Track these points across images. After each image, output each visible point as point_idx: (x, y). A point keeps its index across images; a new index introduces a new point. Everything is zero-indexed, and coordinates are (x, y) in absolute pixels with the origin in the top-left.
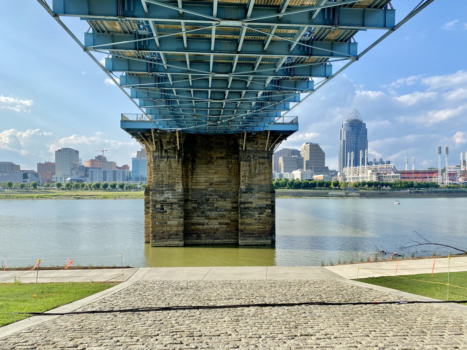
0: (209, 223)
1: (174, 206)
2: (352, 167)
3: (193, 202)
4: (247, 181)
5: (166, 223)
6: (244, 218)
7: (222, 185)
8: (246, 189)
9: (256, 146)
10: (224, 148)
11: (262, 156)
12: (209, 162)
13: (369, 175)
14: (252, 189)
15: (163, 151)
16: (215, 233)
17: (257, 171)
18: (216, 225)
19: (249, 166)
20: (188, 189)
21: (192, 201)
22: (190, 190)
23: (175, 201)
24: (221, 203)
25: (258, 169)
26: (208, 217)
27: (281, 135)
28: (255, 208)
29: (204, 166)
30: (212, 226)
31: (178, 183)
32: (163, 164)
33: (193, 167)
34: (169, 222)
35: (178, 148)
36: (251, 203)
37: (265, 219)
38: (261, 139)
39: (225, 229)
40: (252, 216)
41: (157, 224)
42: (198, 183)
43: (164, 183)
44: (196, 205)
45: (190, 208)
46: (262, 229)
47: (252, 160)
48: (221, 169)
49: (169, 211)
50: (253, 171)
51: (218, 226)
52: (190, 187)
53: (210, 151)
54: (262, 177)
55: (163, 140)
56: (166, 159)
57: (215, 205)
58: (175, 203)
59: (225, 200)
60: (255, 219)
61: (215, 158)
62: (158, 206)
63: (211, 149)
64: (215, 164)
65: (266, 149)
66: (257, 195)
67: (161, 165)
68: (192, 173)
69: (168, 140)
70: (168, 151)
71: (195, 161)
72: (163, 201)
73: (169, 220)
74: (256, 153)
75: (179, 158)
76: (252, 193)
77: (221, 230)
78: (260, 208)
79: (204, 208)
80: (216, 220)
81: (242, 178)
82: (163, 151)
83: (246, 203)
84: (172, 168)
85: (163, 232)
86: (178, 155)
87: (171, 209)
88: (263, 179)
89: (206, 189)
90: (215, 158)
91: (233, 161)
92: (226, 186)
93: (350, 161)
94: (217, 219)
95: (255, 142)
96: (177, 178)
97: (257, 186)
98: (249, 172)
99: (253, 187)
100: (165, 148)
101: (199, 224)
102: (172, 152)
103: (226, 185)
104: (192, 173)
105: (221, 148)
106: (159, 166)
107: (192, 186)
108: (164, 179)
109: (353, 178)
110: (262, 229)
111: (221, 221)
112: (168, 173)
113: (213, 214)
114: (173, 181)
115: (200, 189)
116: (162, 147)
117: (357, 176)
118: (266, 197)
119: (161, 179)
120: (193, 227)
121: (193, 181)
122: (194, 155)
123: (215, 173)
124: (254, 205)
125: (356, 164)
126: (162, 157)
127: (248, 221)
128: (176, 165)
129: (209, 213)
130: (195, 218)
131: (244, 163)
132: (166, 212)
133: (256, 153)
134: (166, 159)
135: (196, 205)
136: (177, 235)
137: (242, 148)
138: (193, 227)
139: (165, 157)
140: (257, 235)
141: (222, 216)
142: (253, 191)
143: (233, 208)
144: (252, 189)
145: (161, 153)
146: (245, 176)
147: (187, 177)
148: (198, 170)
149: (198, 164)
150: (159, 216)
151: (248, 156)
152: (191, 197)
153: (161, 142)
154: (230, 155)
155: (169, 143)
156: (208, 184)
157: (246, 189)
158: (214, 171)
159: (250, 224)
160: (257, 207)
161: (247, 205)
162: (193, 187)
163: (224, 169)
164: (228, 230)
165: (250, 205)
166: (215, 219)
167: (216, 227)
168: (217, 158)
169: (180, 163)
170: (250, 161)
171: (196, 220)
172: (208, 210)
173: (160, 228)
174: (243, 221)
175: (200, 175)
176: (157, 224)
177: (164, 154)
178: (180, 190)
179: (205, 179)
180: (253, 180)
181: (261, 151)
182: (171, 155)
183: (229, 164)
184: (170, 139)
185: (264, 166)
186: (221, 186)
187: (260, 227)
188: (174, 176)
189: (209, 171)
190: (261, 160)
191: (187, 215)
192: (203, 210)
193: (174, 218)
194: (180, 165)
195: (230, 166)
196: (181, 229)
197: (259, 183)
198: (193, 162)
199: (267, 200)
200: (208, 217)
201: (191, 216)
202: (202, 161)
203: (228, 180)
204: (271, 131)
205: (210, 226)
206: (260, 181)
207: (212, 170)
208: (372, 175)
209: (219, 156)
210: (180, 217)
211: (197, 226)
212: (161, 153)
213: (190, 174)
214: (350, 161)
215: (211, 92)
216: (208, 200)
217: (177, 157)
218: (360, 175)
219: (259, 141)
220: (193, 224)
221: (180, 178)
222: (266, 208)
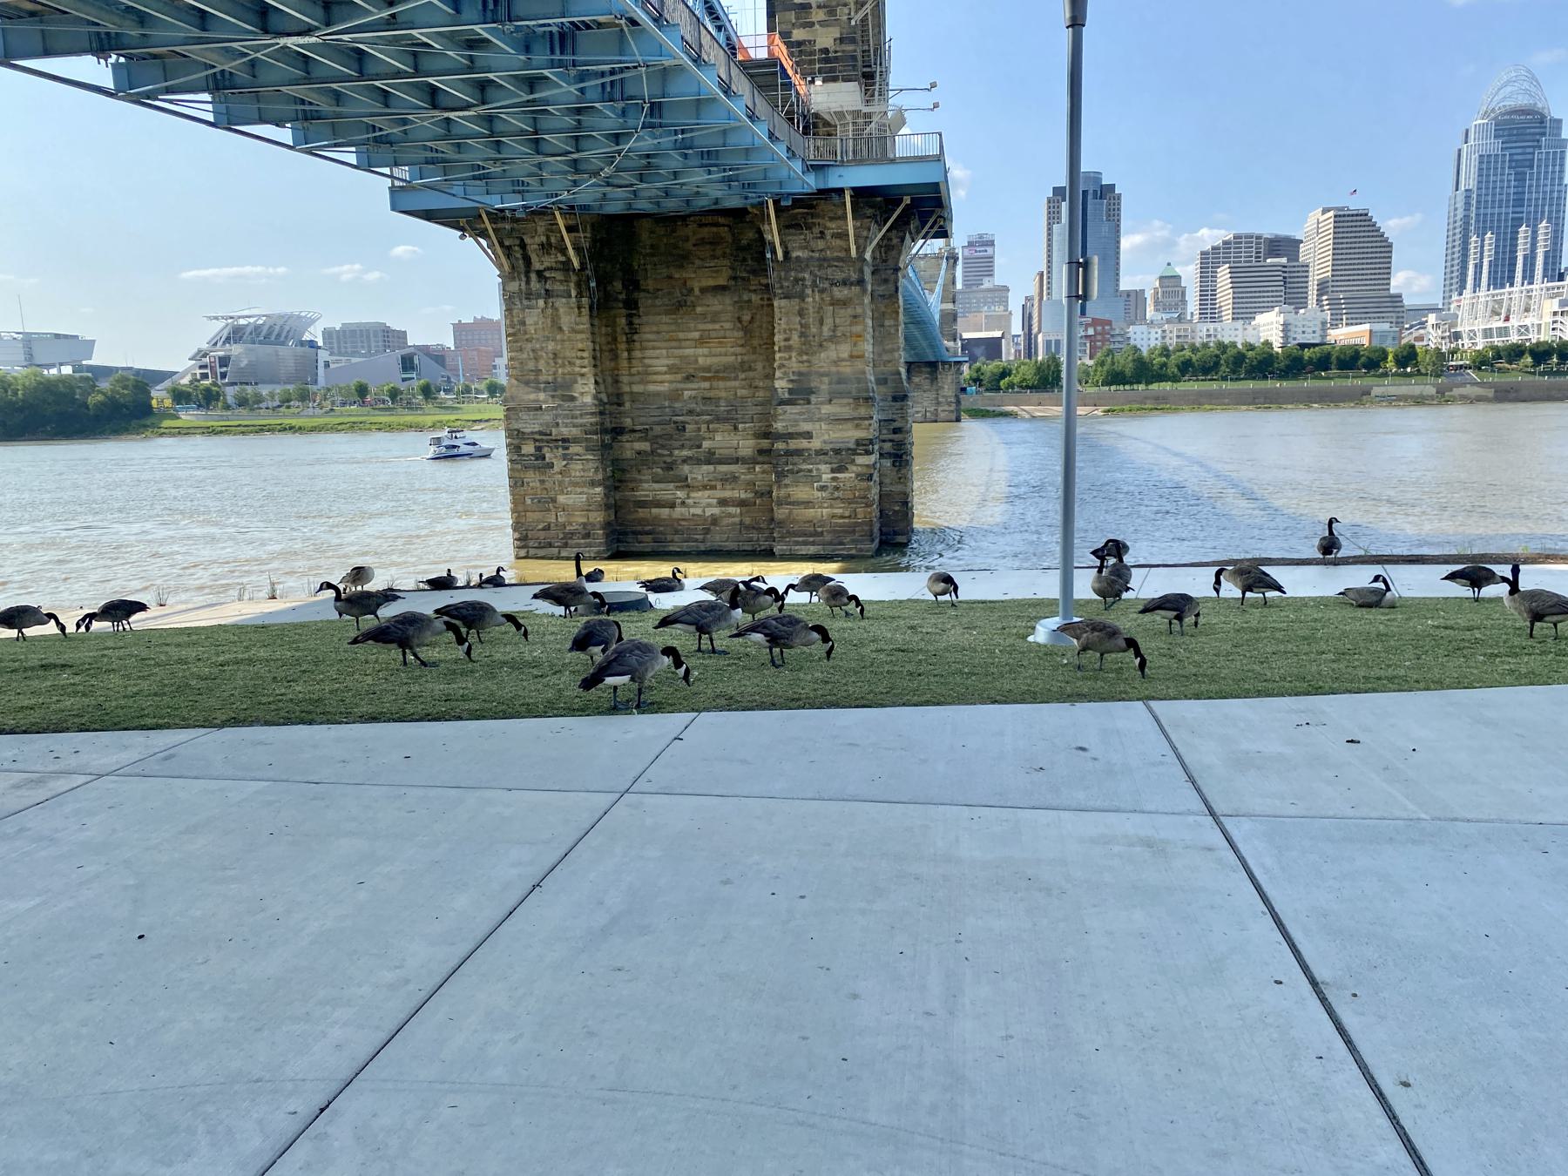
0: (690, 501)
1: (575, 449)
2: (1483, 292)
3: (638, 435)
4: (794, 365)
5: (554, 500)
6: (786, 486)
7: (723, 379)
8: (791, 391)
9: (821, 244)
10: (724, 255)
11: (839, 276)
12: (680, 306)
13: (1548, 319)
14: (811, 392)
15: (533, 276)
16: (707, 531)
17: (825, 328)
18: (709, 505)
19: (801, 313)
20: (619, 395)
21: (634, 431)
22: (626, 398)
23: (575, 432)
24: (721, 440)
25: (829, 322)
26: (683, 482)
27: (907, 200)
29: (665, 319)
30: (698, 511)
31: (583, 375)
32: (534, 318)
33: (630, 324)
34: (561, 499)
35: (576, 264)
36: (808, 435)
37: (853, 489)
38: (831, 219)
39: (737, 520)
40: (811, 478)
41: (529, 501)
42: (646, 373)
43: (542, 378)
44: (645, 446)
45: (628, 454)
46: (842, 517)
47: (809, 291)
48: (717, 326)
49: (559, 464)
51: (716, 511)
52: (626, 389)
53: (682, 266)
54: (844, 350)
55: (527, 240)
56: (541, 303)
57: (706, 444)
58: (576, 441)
59: (736, 428)
60: (822, 488)
61: (697, 291)
62: (529, 448)
63: (683, 259)
64: (699, 309)
65: (853, 253)
66: (826, 409)
67: (529, 321)
68: (630, 341)
69: (544, 239)
70: (547, 274)
71: (636, 303)
72: (541, 433)
73: (562, 493)
74: (820, 267)
75: (580, 295)
76: (809, 403)
77: (726, 521)
78: (837, 452)
79: (671, 455)
80: (707, 493)
81: (777, 356)
82: (533, 276)
83: (791, 436)
84: (560, 329)
85: (547, 528)
86: (578, 285)
87: (565, 457)
88: (845, 355)
89: (675, 396)
90: (697, 291)
91: (754, 297)
92: (736, 383)
93: (1478, 267)
94: (713, 488)
95: (816, 230)
96: (578, 362)
97: (826, 380)
98: (802, 335)
100: (537, 265)
101: (659, 504)
102: (559, 276)
103: (736, 379)
104: (630, 341)
105: (714, 257)
106: (523, 323)
107: (630, 384)
108: (542, 365)
109: (1487, 333)
110: (842, 517)
111: (727, 494)
112: (551, 346)
113: (700, 473)
114: (568, 369)
115: (658, 394)
116: (527, 260)
117: (1501, 324)
118: (856, 414)
119: (531, 365)
120: (642, 513)
121: (634, 371)
122: (632, 284)
123: (701, 342)
124: (816, 444)
125: (1502, 275)
126: (529, 295)
127: (801, 492)
128: (572, 316)
129: (686, 468)
130: (646, 485)
131: (784, 302)
132: (551, 466)
133: (820, 267)
134: (541, 303)
135: (645, 446)
136: (587, 536)
137: (774, 252)
138: (642, 513)
139: (539, 297)
140: (828, 538)
141: (732, 479)
142: (813, 398)
143: (761, 452)
144: (811, 392)
145: (528, 282)
146: (789, 348)
147: (615, 357)
148: (647, 334)
149: (647, 314)
150: (532, 478)
151: (797, 280)
152: (629, 420)
153: (523, 246)
154: (743, 279)
155: (546, 248)
156: (679, 377)
157: (791, 391)
158: (696, 335)
159: (808, 504)
160: (828, 447)
161: (794, 444)
162: (637, 388)
163: (727, 325)
164: (747, 521)
165: (804, 444)
166: (705, 487)
167: (709, 512)
168: (703, 290)
169: (585, 311)
170: (802, 297)
171: (648, 489)
172: (684, 461)
173: (537, 516)
174: (783, 492)
175: (654, 348)
176: (529, 501)
177: (535, 285)
178: (588, 399)
179: (670, 362)
180: (815, 360)
181: (839, 259)
182: (559, 287)
183: (741, 308)
184: (548, 238)
185: (850, 311)
186: (721, 384)
188: (568, 354)
189: (681, 336)
190: (840, 293)
191: (617, 478)
192: (669, 460)
193: (576, 484)
194: (586, 319)
195: (746, 318)
196: (598, 517)
197: (834, 369)
198: (631, 305)
199: (857, 426)
200: (683, 482)
201: (634, 480)
202: (658, 302)
203: (743, 362)
204: (853, 189)
205: (692, 511)
206: (836, 363)
207: (690, 331)
208: (1559, 318)
209: (711, 283)
210: (593, 484)
211: (655, 511)
212: (528, 282)
213: (623, 346)
214: (1478, 267)
216: (681, 428)
217: (574, 293)
218: (1514, 322)
219: (829, 224)
220: (643, 504)
221: (586, 362)
222: (854, 452)
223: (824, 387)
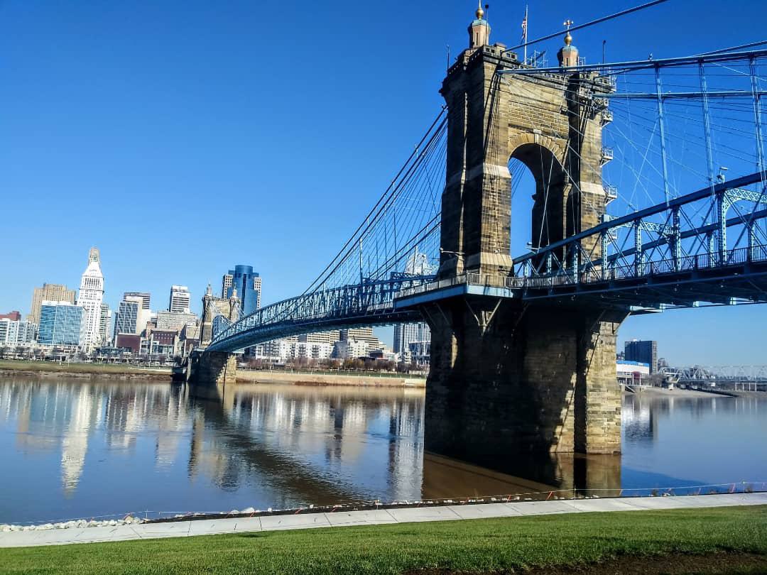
8: (593, 386)
28: (604, 413)
36: (599, 405)
40: (600, 423)
50: (600, 360)
78: (610, 413)
88: (610, 372)
99: (600, 384)
124: (602, 409)
144: (599, 386)
160: (606, 411)
161: (596, 408)
187: (610, 439)
195: (567, 353)
197: (606, 378)
199: (617, 402)
215: (561, 238)
223: (604, 385)
